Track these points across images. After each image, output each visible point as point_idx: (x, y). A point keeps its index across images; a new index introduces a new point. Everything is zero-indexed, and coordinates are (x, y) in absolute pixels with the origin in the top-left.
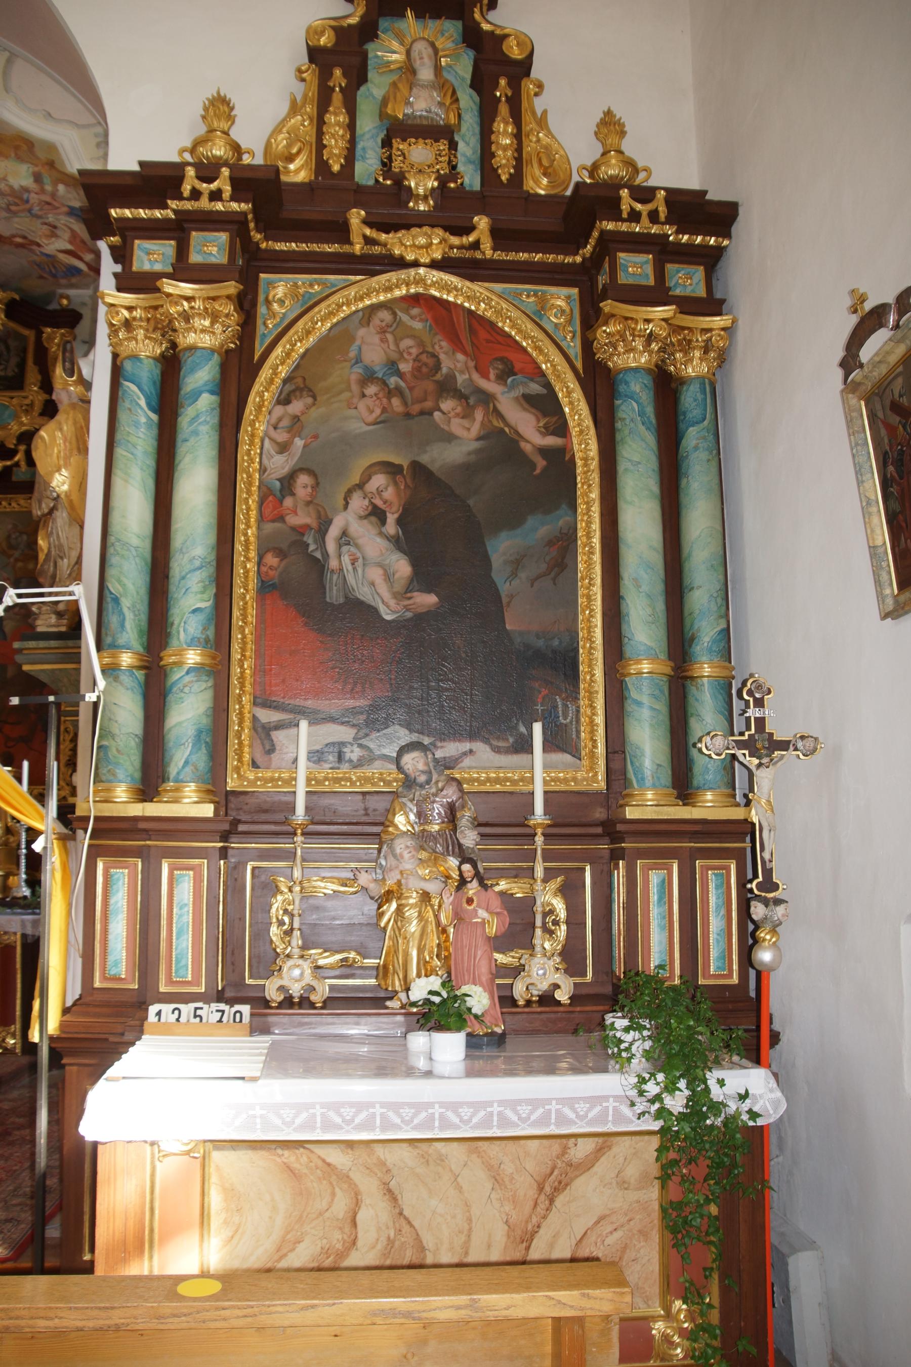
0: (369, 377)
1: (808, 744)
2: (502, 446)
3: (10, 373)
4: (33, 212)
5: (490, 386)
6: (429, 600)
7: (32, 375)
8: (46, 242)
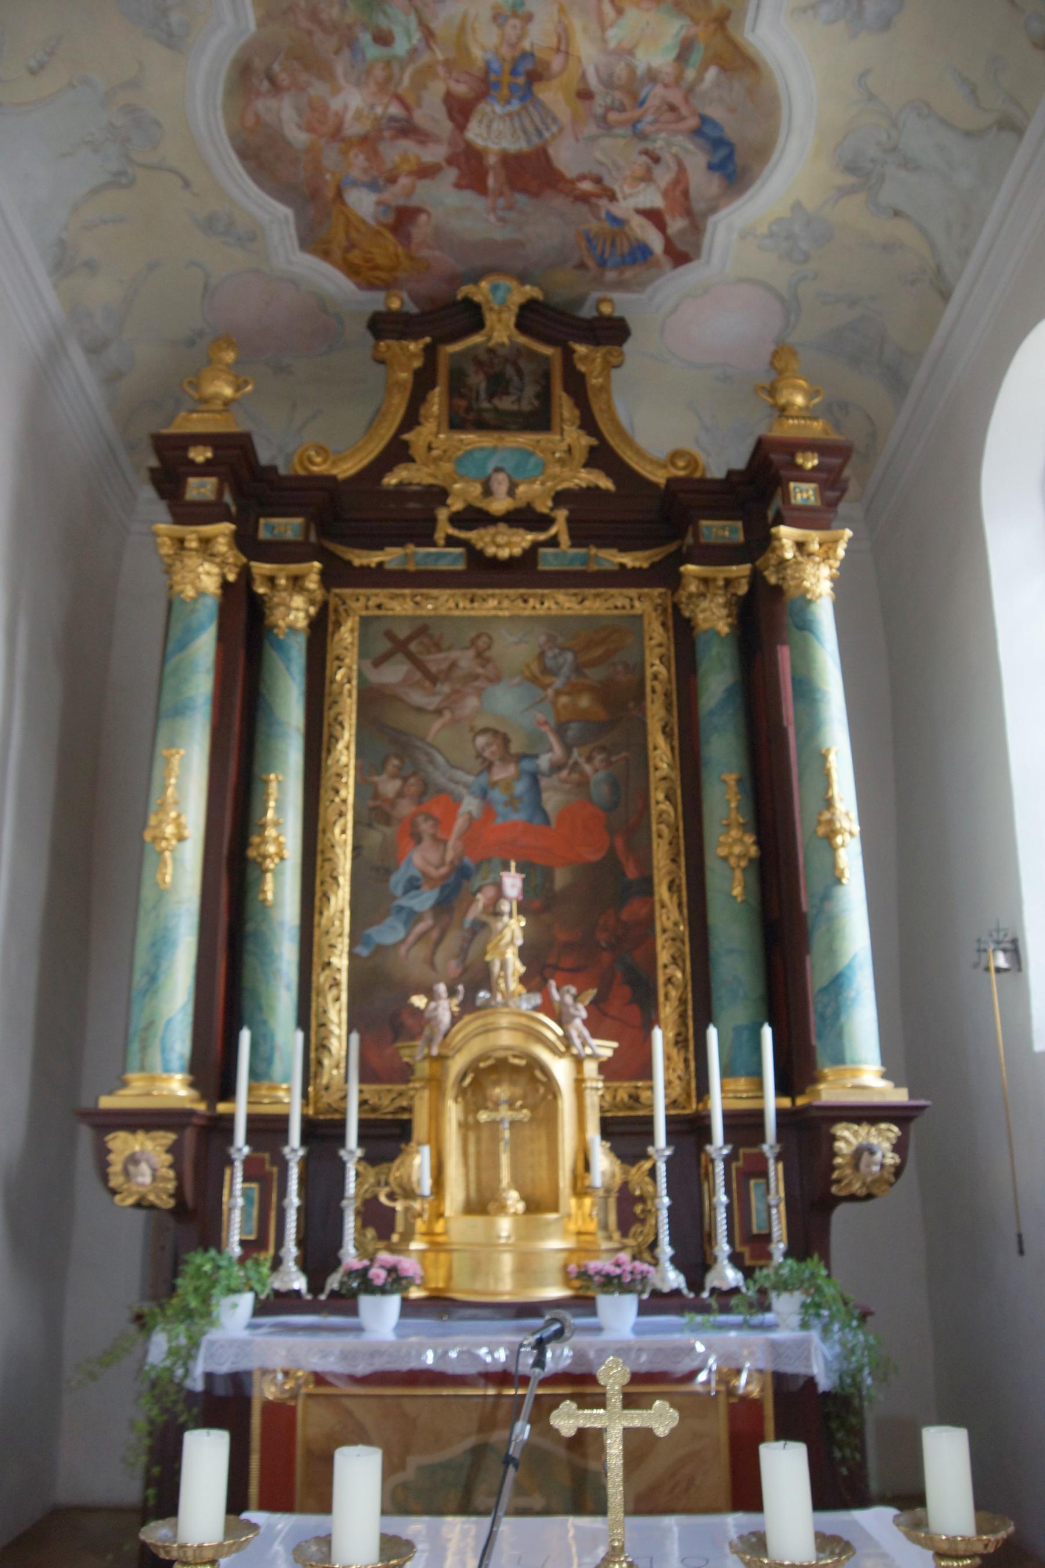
3: (526, 407)
4: (640, 126)
7: (565, 407)
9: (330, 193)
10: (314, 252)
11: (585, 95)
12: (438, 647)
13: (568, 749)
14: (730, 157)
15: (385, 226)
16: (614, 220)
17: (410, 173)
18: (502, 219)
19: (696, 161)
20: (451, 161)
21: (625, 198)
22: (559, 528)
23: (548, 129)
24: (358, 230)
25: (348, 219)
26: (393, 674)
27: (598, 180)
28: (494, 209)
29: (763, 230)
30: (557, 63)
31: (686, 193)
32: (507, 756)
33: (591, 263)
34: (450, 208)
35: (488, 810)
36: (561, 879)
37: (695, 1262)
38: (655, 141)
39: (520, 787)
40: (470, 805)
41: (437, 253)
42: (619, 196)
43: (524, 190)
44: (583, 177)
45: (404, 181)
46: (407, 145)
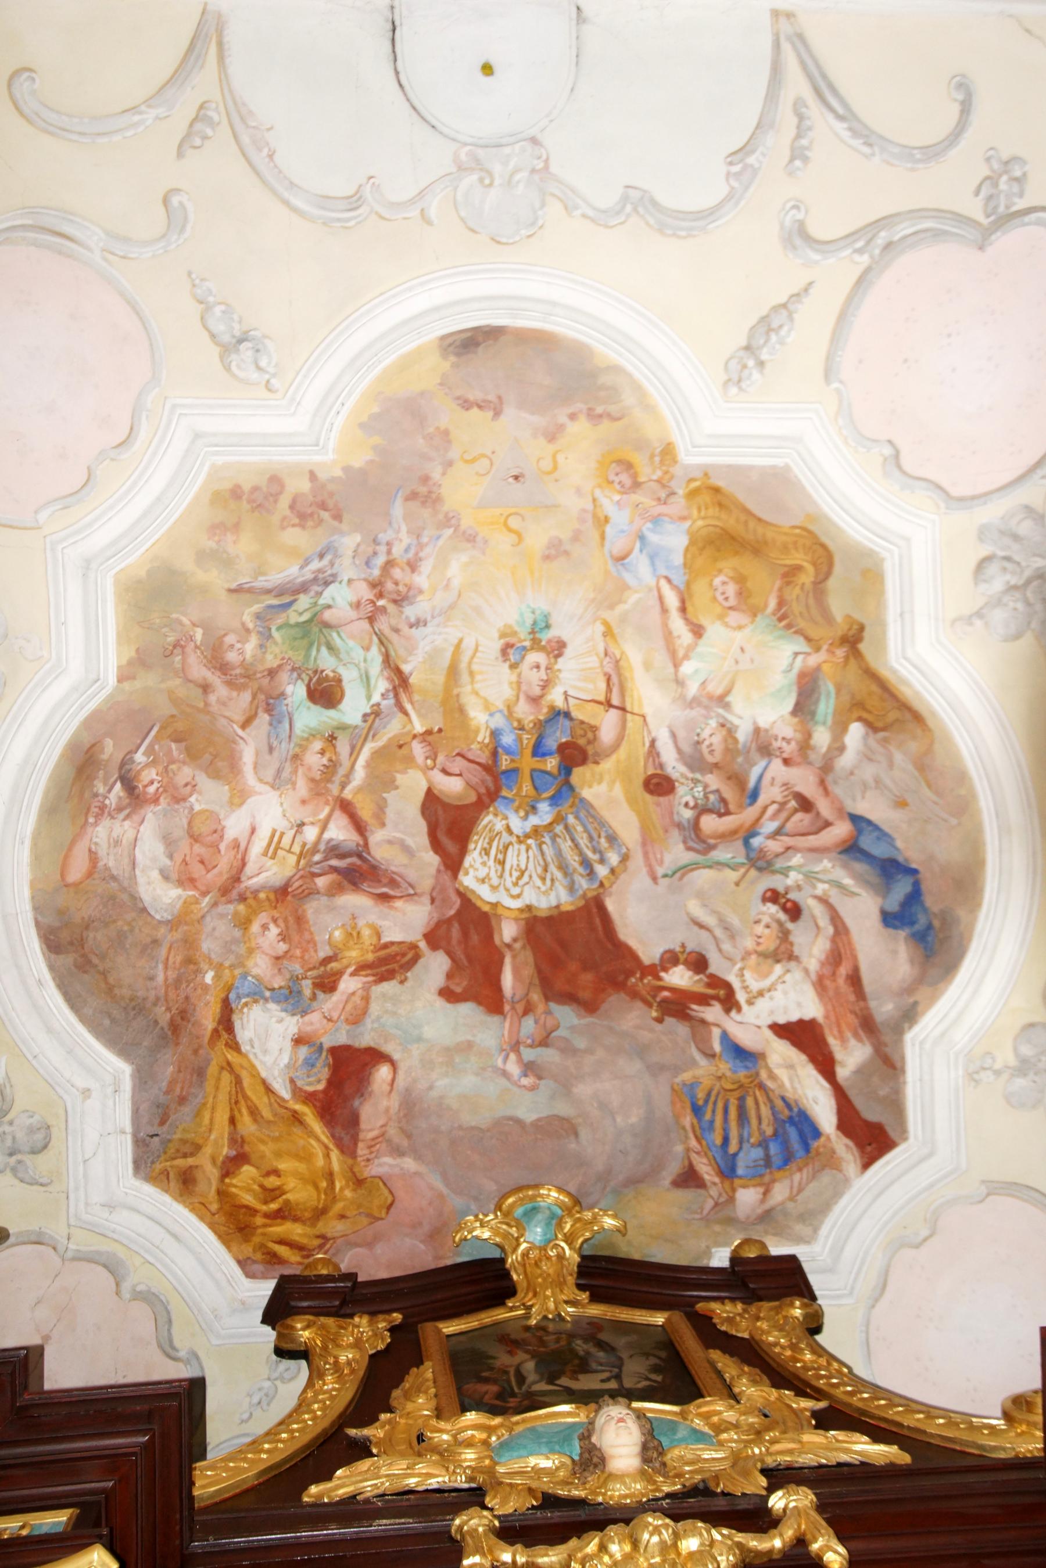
8: (755, 985)
9: (208, 1018)
10: (159, 1178)
11: (659, 785)
14: (915, 896)
15: (309, 1098)
16: (740, 1053)
17: (361, 968)
18: (528, 1068)
19: (864, 910)
20: (434, 938)
21: (750, 1003)
23: (602, 861)
24: (254, 1112)
25: (238, 1081)
27: (699, 964)
28: (516, 1046)
29: (1006, 1057)
30: (607, 724)
31: (855, 980)
33: (705, 1170)
34: (439, 1047)
38: (785, 872)
41: (409, 1164)
42: (741, 997)
43: (569, 998)
44: (671, 959)
45: (348, 984)
46: (355, 901)
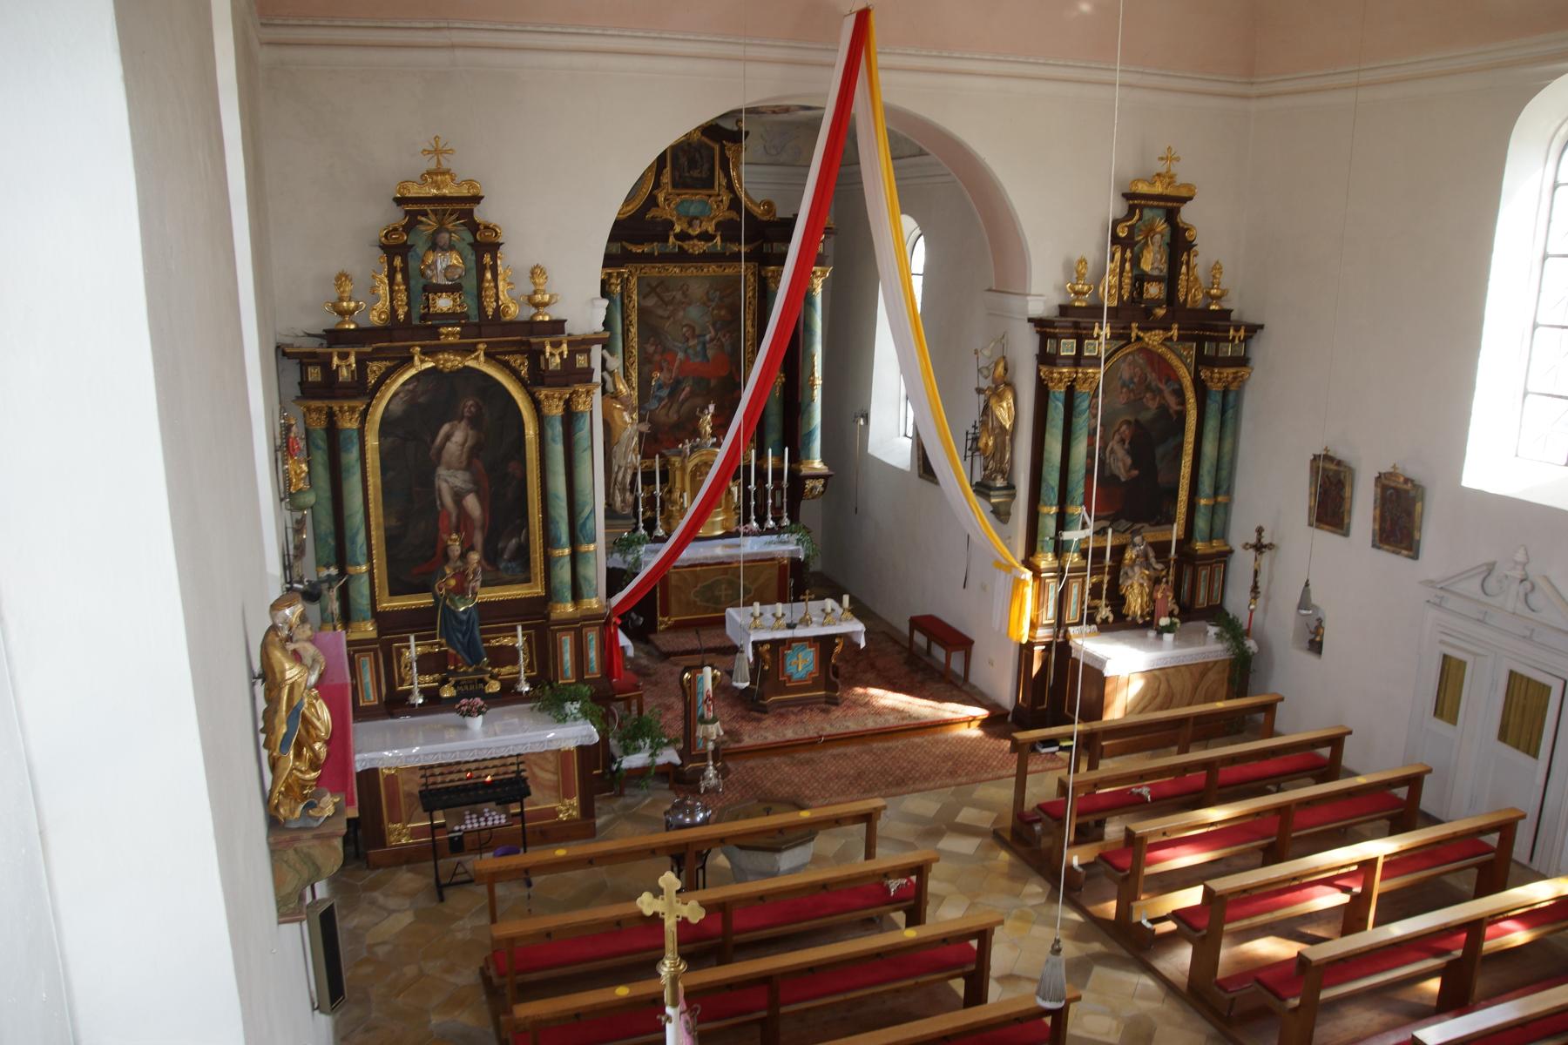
0: (1124, 385)
1: (1270, 546)
2: (1163, 409)
5: (1162, 386)
6: (1135, 472)
12: (667, 290)
13: (717, 331)
22: (718, 239)
26: (651, 302)
32: (694, 336)
35: (687, 358)
36: (713, 383)
37: (761, 520)
39: (699, 348)
40: (681, 355)
